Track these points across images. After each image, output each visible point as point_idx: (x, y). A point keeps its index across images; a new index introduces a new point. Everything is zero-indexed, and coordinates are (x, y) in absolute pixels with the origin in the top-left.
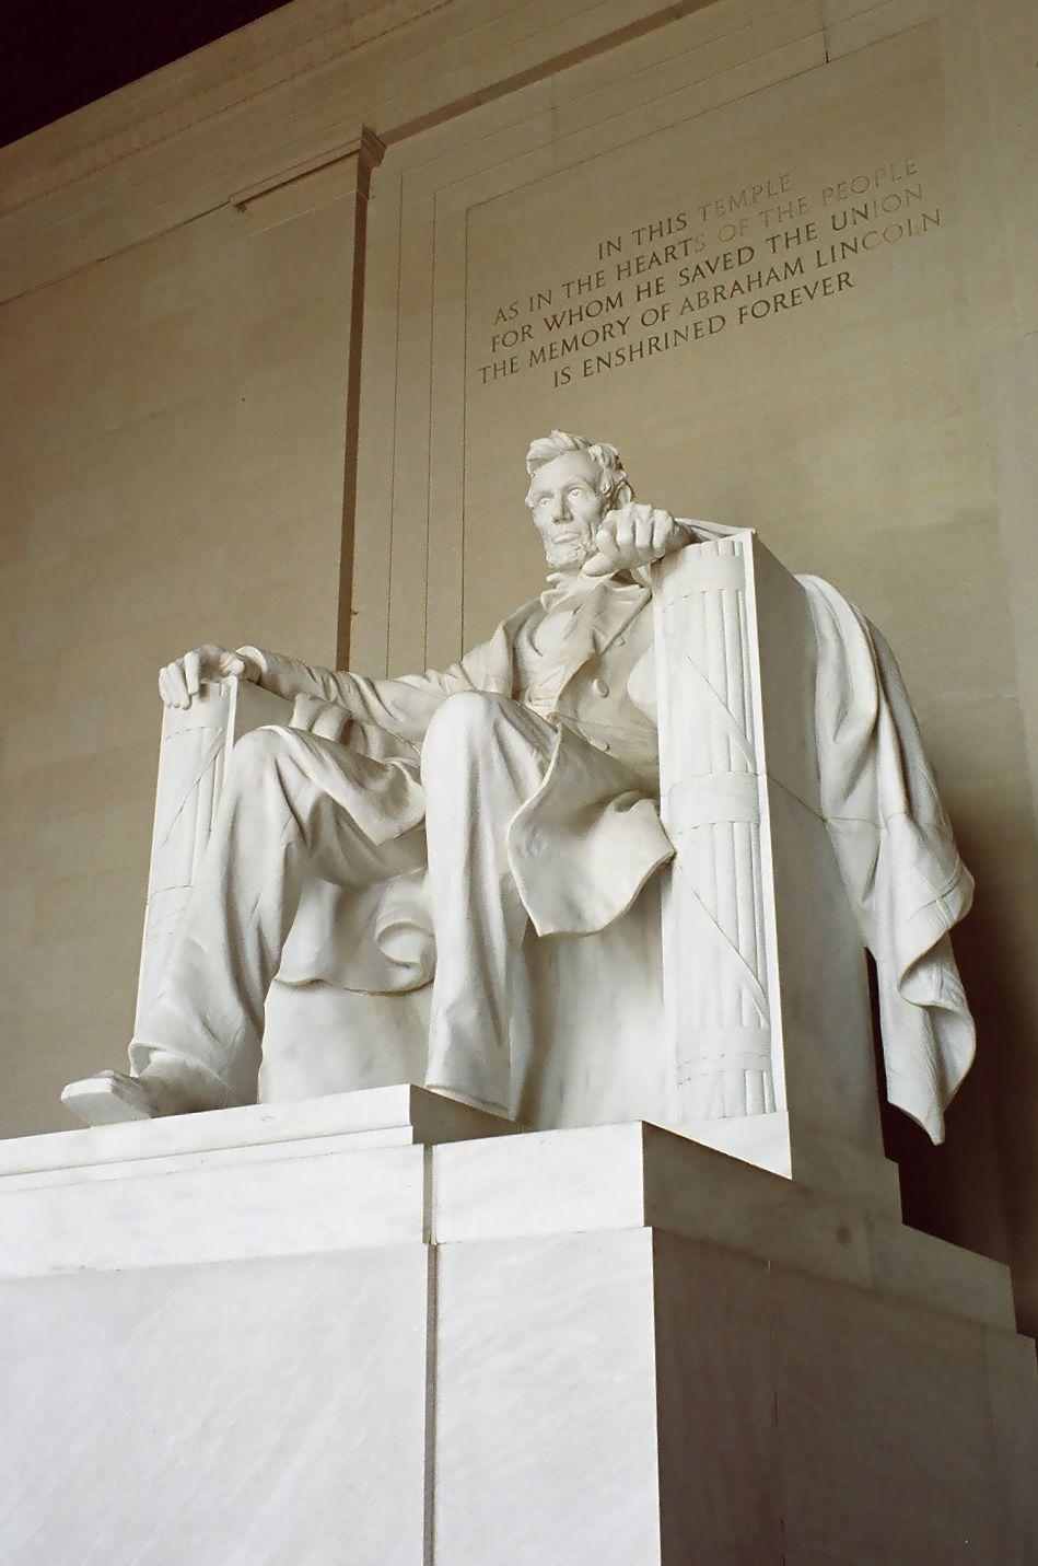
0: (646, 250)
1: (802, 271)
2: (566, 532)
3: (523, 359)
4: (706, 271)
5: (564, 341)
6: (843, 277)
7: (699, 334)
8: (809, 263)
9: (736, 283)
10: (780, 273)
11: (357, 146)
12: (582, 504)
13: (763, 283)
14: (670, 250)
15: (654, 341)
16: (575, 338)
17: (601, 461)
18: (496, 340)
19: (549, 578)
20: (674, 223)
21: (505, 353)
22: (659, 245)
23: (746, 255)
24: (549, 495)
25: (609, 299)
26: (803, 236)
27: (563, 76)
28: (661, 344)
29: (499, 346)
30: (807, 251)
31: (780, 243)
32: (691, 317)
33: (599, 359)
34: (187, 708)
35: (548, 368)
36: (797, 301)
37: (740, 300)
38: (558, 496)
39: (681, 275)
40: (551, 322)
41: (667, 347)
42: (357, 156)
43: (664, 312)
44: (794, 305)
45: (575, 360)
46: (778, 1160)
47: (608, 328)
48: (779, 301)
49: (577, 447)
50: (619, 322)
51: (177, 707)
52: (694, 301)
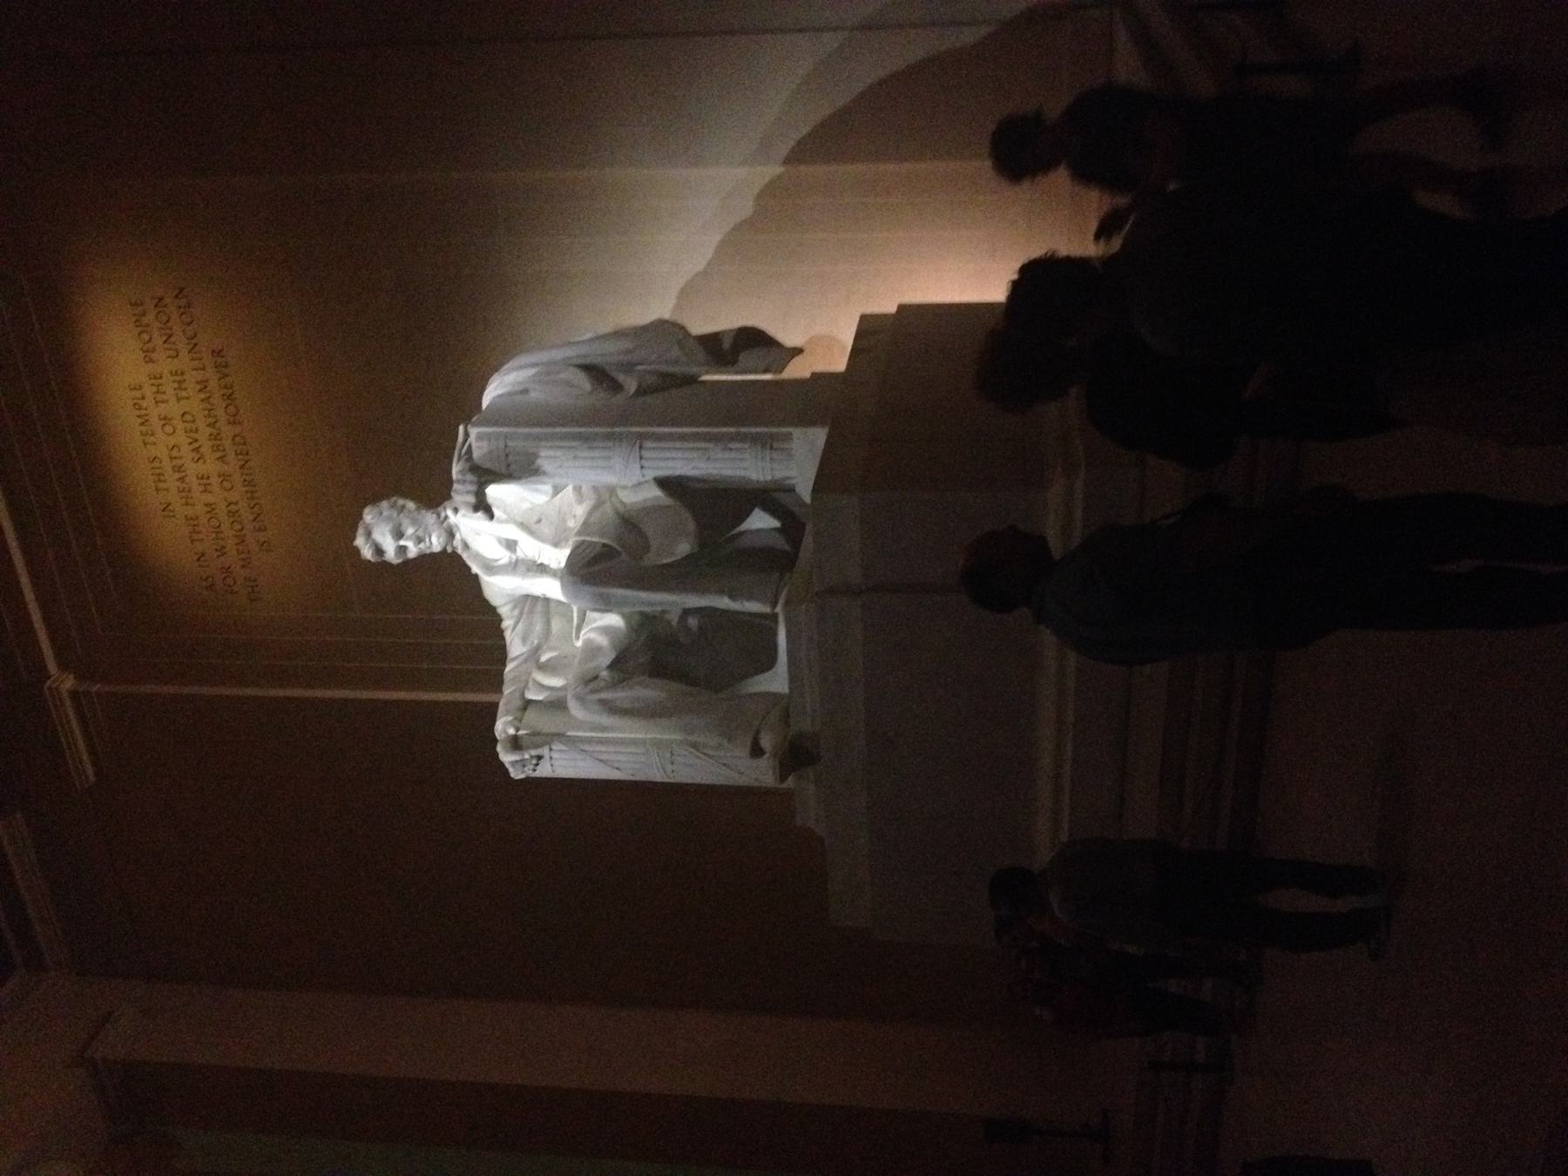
4: (196, 445)
8: (199, 375)
19: (449, 550)
37: (222, 423)
38: (402, 543)
46: (819, 435)
52: (219, 454)
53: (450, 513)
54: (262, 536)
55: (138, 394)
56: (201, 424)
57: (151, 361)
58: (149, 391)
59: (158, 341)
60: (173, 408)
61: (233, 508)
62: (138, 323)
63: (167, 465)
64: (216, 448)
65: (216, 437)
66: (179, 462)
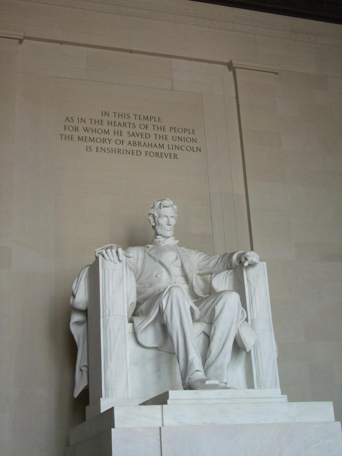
0: (118, 120)
1: (164, 148)
2: (170, 228)
3: (75, 138)
5: (90, 138)
6: (175, 155)
7: (133, 154)
8: (166, 146)
9: (145, 143)
10: (158, 145)
11: (22, 38)
12: (173, 221)
13: (153, 146)
14: (125, 124)
15: (119, 150)
16: (94, 138)
17: (176, 211)
18: (66, 127)
19: (158, 237)
20: (126, 116)
21: (67, 133)
22: (122, 120)
23: (148, 136)
24: (167, 217)
25: (105, 130)
26: (164, 137)
27: (90, 49)
28: (122, 152)
29: (67, 129)
30: (166, 143)
31: (158, 137)
32: (130, 148)
33: (102, 148)
34: (116, 263)
35: (84, 144)
36: (162, 156)
39: (128, 133)
40: (85, 129)
41: (123, 154)
42: (18, 40)
43: (122, 142)
44: (161, 157)
45: (94, 145)
47: (104, 140)
48: (157, 154)
49: (172, 206)
50: (108, 139)
51: (111, 262)
53: (177, 241)
54: (94, 149)
55: (157, 119)
56: (147, 141)
57: (171, 129)
58: (159, 124)
59: (178, 134)
60: (150, 130)
61: (107, 141)
62: (185, 130)
63: (126, 120)
64: (134, 143)
65: (140, 144)
66: (128, 125)
